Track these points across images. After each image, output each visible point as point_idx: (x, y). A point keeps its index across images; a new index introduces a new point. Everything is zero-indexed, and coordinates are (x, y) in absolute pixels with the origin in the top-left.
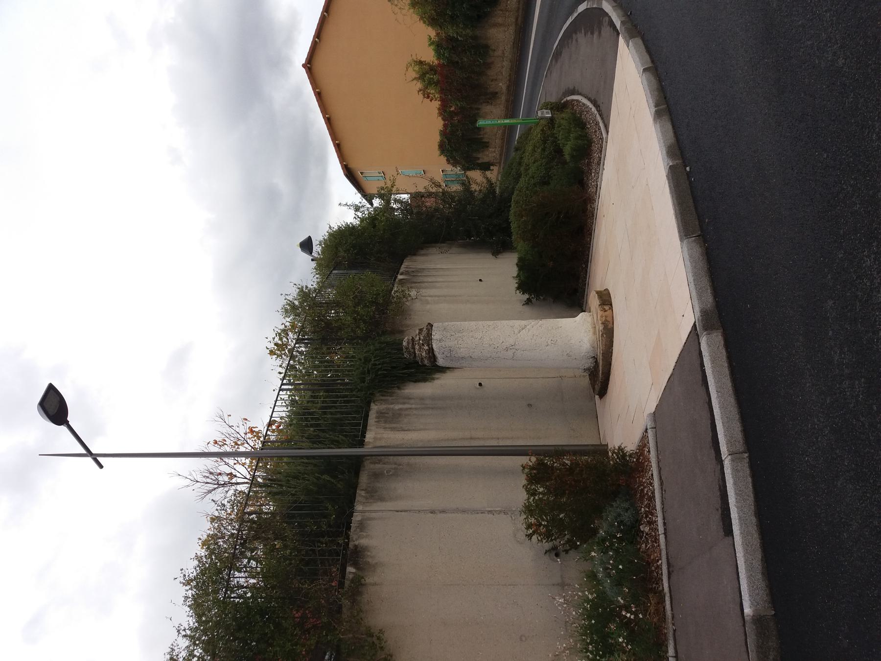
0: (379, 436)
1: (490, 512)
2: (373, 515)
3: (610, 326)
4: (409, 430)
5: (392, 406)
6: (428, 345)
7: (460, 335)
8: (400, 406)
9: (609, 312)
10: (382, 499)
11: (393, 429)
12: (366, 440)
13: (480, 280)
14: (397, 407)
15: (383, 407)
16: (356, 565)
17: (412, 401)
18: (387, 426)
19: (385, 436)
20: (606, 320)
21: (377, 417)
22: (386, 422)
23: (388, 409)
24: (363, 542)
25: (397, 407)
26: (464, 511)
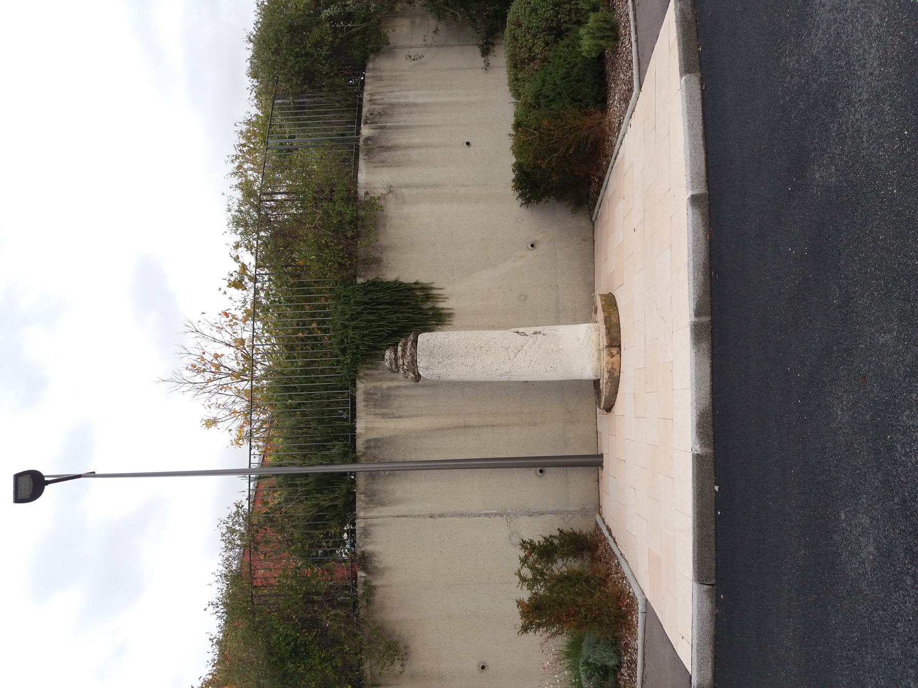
0: (370, 425)
1: (487, 515)
2: (375, 521)
3: (616, 374)
5: (379, 384)
6: (414, 373)
7: (449, 362)
8: (389, 384)
10: (382, 504)
11: (384, 416)
12: (358, 431)
13: (468, 144)
15: (370, 385)
16: (365, 569)
18: (378, 411)
19: (376, 425)
20: (612, 368)
21: (366, 400)
22: (375, 406)
23: (375, 388)
24: (369, 548)
25: (386, 385)
26: (462, 515)
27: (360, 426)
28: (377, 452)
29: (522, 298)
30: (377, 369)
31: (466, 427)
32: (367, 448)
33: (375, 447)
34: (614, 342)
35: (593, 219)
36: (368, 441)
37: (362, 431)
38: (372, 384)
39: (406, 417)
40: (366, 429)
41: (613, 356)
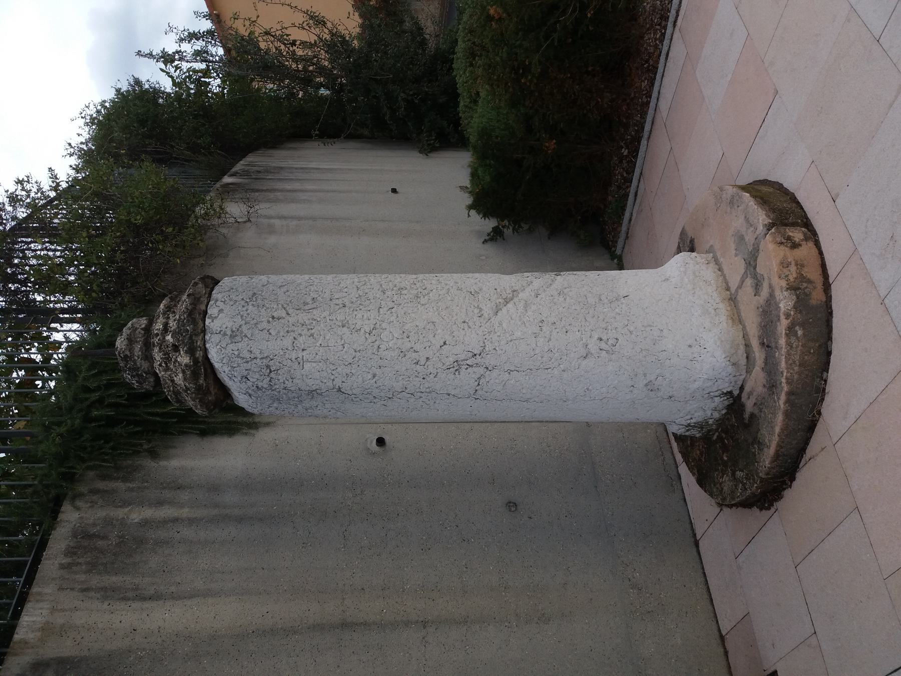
0: (59, 619)
3: (817, 296)
4: (156, 597)
5: (121, 513)
6: (191, 351)
7: (303, 317)
8: (148, 513)
11: (109, 594)
13: (394, 191)
14: (136, 515)
17: (184, 496)
18: (95, 581)
19: (79, 618)
20: (801, 278)
22: (92, 567)
23: (109, 522)
25: (136, 515)
30: (125, 480)
31: (345, 625)
35: (618, 252)
37: (31, 636)
38: (101, 513)
39: (174, 597)
40: (47, 630)
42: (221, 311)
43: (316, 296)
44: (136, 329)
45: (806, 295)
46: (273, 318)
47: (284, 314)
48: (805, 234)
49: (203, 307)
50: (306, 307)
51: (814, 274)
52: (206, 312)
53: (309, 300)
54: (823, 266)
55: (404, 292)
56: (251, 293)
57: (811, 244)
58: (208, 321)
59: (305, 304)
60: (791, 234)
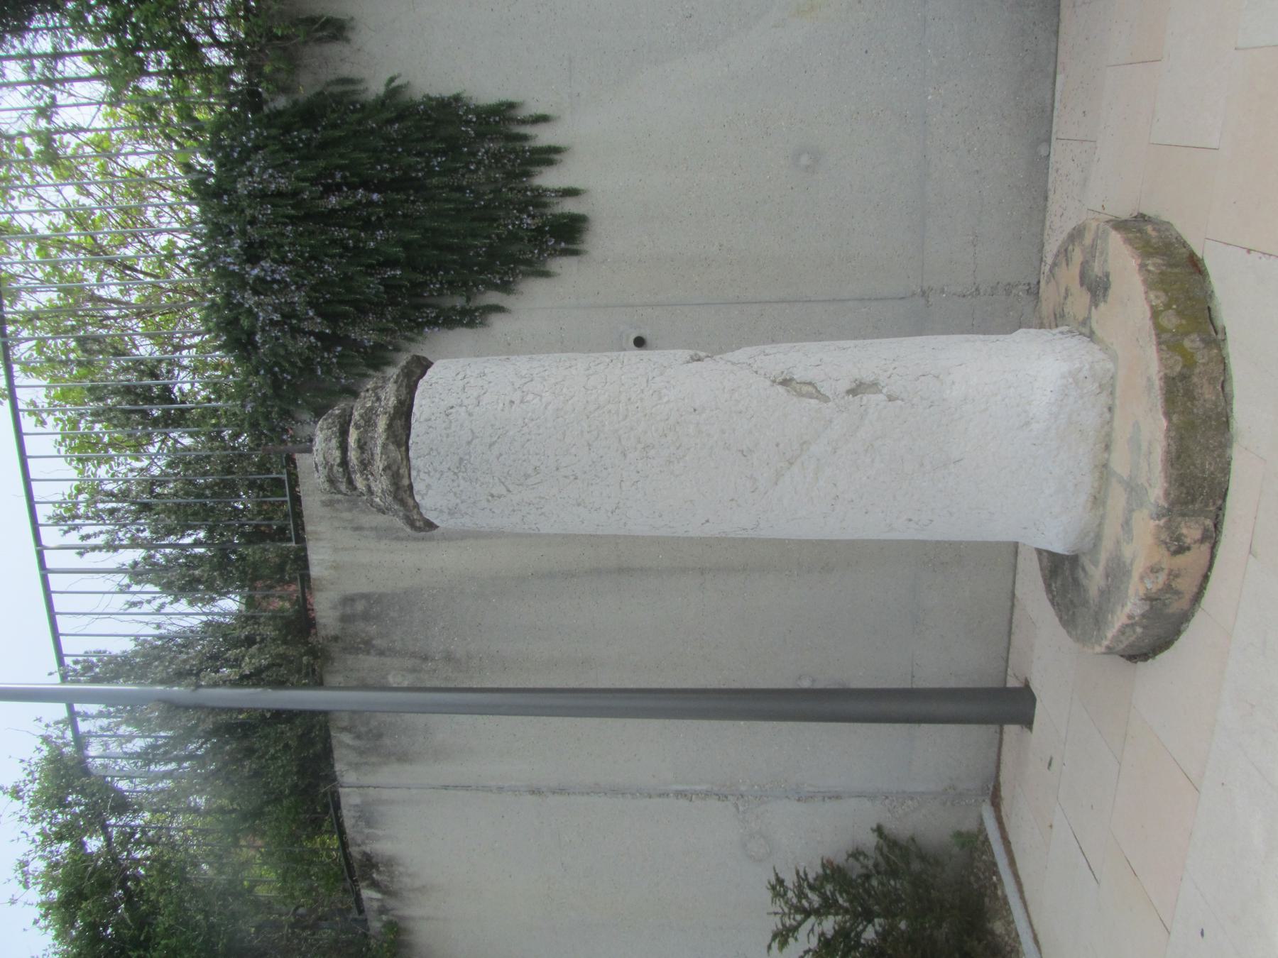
1: (680, 794)
2: (386, 794)
9: (1193, 559)
12: (315, 571)
27: (319, 559)
28: (373, 629)
29: (805, 160)
31: (621, 570)
32: (345, 619)
33: (366, 617)
34: (1199, 489)
36: (348, 600)
41: (1181, 550)
42: (429, 487)
43: (538, 464)
44: (332, 466)
45: (1165, 605)
46: (492, 496)
47: (504, 492)
48: (1206, 530)
49: (405, 482)
50: (529, 481)
51: (1187, 585)
52: (411, 487)
53: (530, 471)
54: (1206, 578)
55: (652, 453)
56: (456, 458)
57: (1205, 548)
58: (417, 498)
59: (527, 476)
60: (1184, 531)
